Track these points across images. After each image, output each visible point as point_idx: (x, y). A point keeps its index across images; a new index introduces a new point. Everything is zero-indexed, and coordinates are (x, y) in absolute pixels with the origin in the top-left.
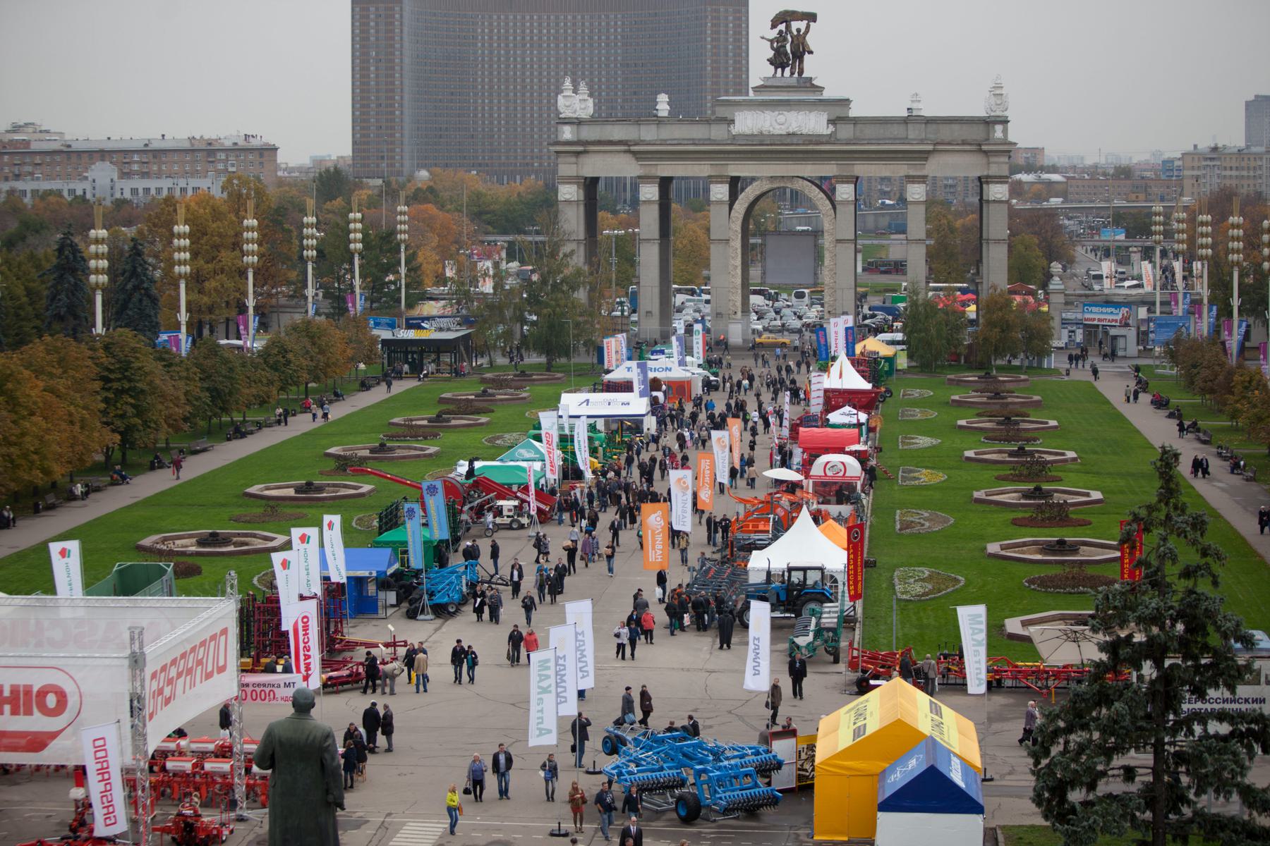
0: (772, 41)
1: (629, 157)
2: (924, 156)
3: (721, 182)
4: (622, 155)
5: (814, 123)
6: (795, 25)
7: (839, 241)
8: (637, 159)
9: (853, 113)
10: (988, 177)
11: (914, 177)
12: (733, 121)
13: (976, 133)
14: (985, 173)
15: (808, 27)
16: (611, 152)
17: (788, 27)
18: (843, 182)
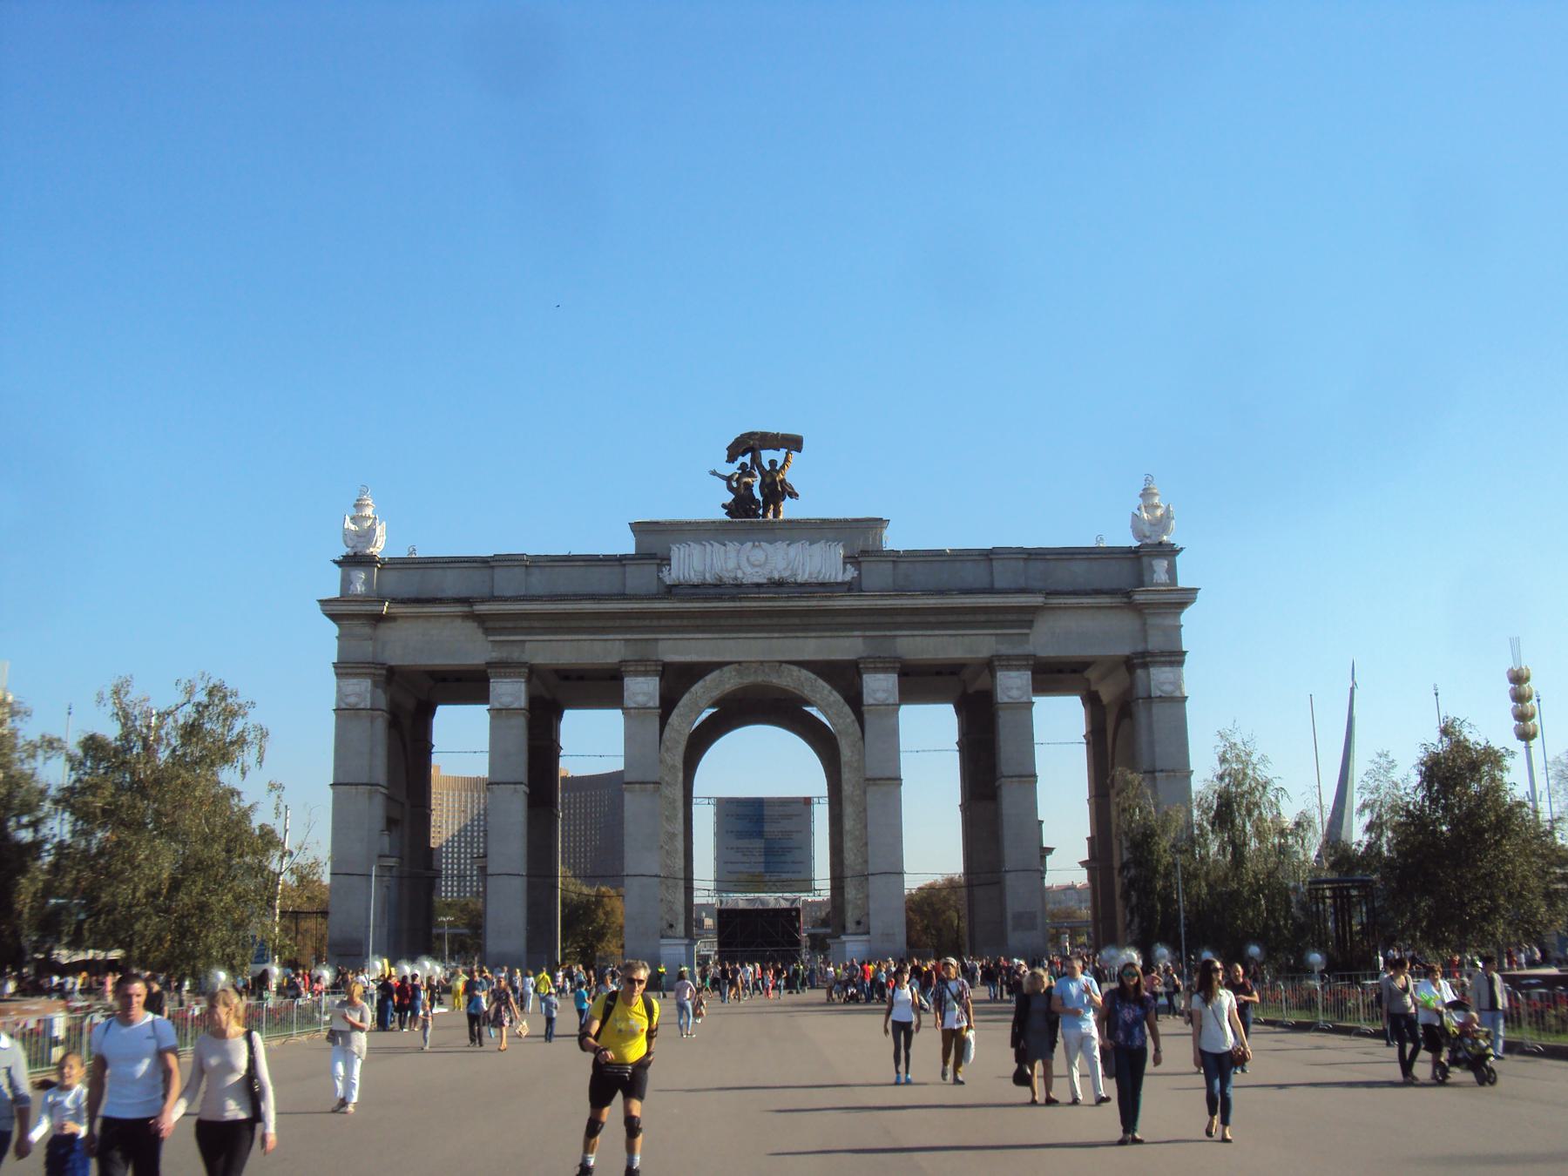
0: (729, 479)
1: (471, 626)
2: (1025, 618)
3: (646, 674)
4: (459, 622)
5: (822, 563)
6: (767, 456)
7: (875, 780)
8: (487, 631)
9: (894, 540)
10: (1144, 654)
11: (1009, 658)
12: (665, 560)
13: (1118, 575)
14: (1140, 648)
15: (786, 460)
16: (439, 616)
17: (756, 461)
18: (876, 670)
